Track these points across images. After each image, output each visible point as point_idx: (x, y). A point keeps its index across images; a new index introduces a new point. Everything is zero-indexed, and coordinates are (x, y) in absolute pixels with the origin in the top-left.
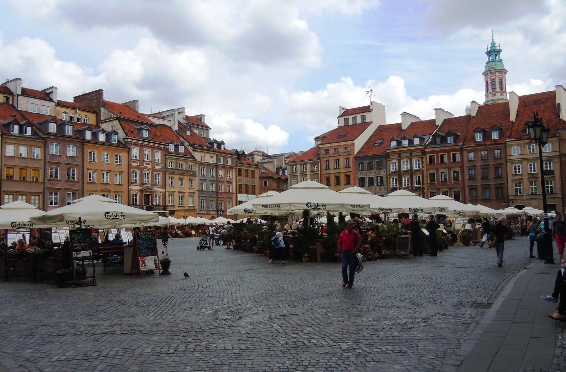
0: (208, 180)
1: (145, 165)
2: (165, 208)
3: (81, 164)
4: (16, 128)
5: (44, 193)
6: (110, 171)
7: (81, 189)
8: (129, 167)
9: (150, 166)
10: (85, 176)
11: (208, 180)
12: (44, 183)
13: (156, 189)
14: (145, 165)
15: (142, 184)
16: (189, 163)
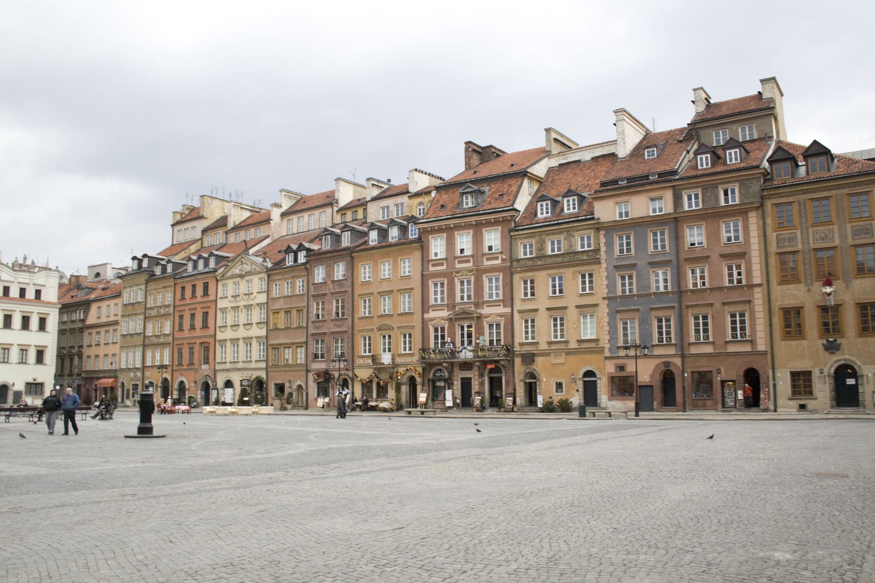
0: (715, 256)
1: (458, 266)
2: (509, 350)
3: (349, 289)
4: (292, 255)
5: (306, 343)
6: (392, 291)
7: (350, 330)
8: (424, 278)
9: (470, 265)
10: (355, 307)
11: (642, 263)
12: (307, 327)
13: (485, 311)
14: (458, 266)
15: (452, 306)
16: (576, 234)
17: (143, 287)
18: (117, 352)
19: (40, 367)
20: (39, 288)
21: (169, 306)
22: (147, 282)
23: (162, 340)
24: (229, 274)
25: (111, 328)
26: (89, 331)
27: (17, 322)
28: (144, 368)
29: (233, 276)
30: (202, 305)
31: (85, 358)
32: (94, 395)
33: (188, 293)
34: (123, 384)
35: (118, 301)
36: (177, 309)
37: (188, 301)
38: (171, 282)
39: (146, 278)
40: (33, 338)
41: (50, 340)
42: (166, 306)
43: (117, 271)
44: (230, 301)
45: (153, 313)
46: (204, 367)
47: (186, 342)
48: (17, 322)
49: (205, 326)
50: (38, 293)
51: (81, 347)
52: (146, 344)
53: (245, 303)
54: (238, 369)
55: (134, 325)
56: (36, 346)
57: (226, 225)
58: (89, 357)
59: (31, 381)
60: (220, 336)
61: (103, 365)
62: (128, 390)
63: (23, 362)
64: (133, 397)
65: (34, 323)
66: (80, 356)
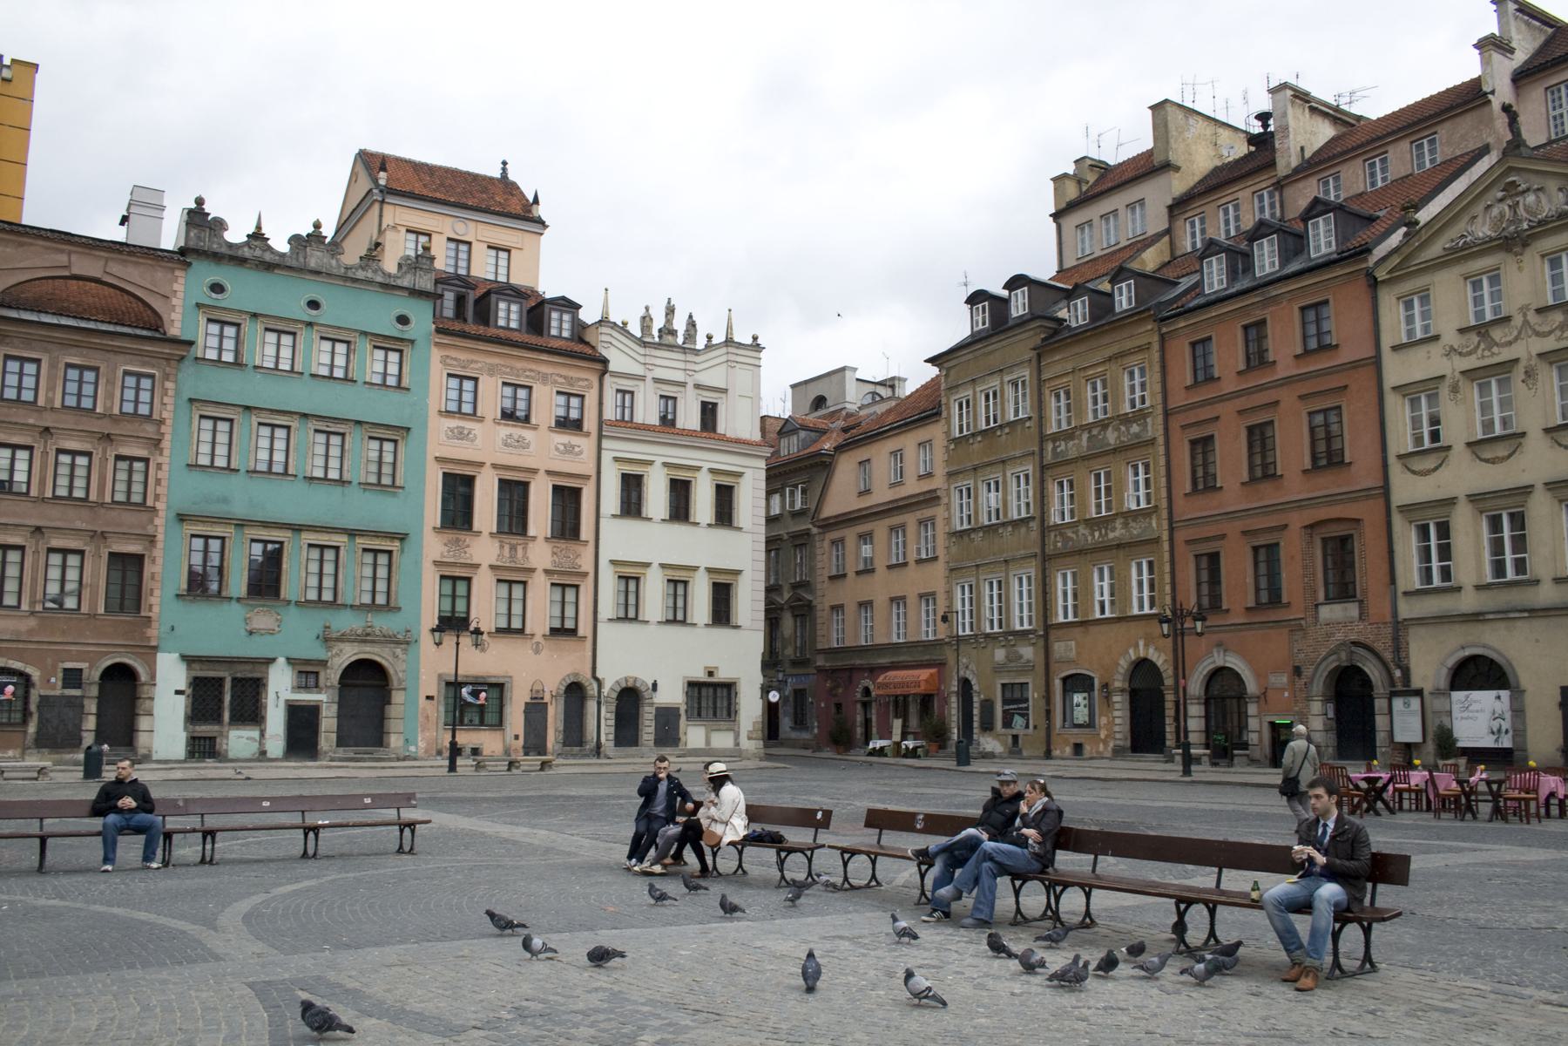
17: (1026, 373)
18: (939, 586)
19: (721, 633)
20: (710, 397)
21: (1140, 416)
22: (1041, 352)
23: (1117, 533)
24: (1435, 250)
25: (910, 519)
26: (835, 535)
27: (656, 497)
28: (1047, 630)
29: (1459, 254)
30: (1305, 388)
31: (822, 613)
32: (859, 718)
33: (1228, 355)
34: (965, 684)
35: (935, 432)
36: (1175, 424)
37: (1229, 385)
38: (1147, 333)
39: (1037, 341)
40: (701, 547)
41: (743, 552)
42: (1126, 420)
43: (871, 388)
44: (1451, 351)
45: (1071, 449)
46: (1328, 612)
47: (1233, 529)
48: (656, 497)
49: (1328, 456)
50: (709, 412)
51: (804, 585)
52: (1051, 551)
53: (1550, 344)
54: (1534, 613)
55: (1007, 496)
56: (710, 570)
57: (1272, 164)
58: (837, 608)
59: (700, 675)
60: (1407, 488)
61: (888, 630)
62: (987, 706)
63: (677, 618)
64: (1007, 723)
65: (703, 501)
66: (804, 611)
